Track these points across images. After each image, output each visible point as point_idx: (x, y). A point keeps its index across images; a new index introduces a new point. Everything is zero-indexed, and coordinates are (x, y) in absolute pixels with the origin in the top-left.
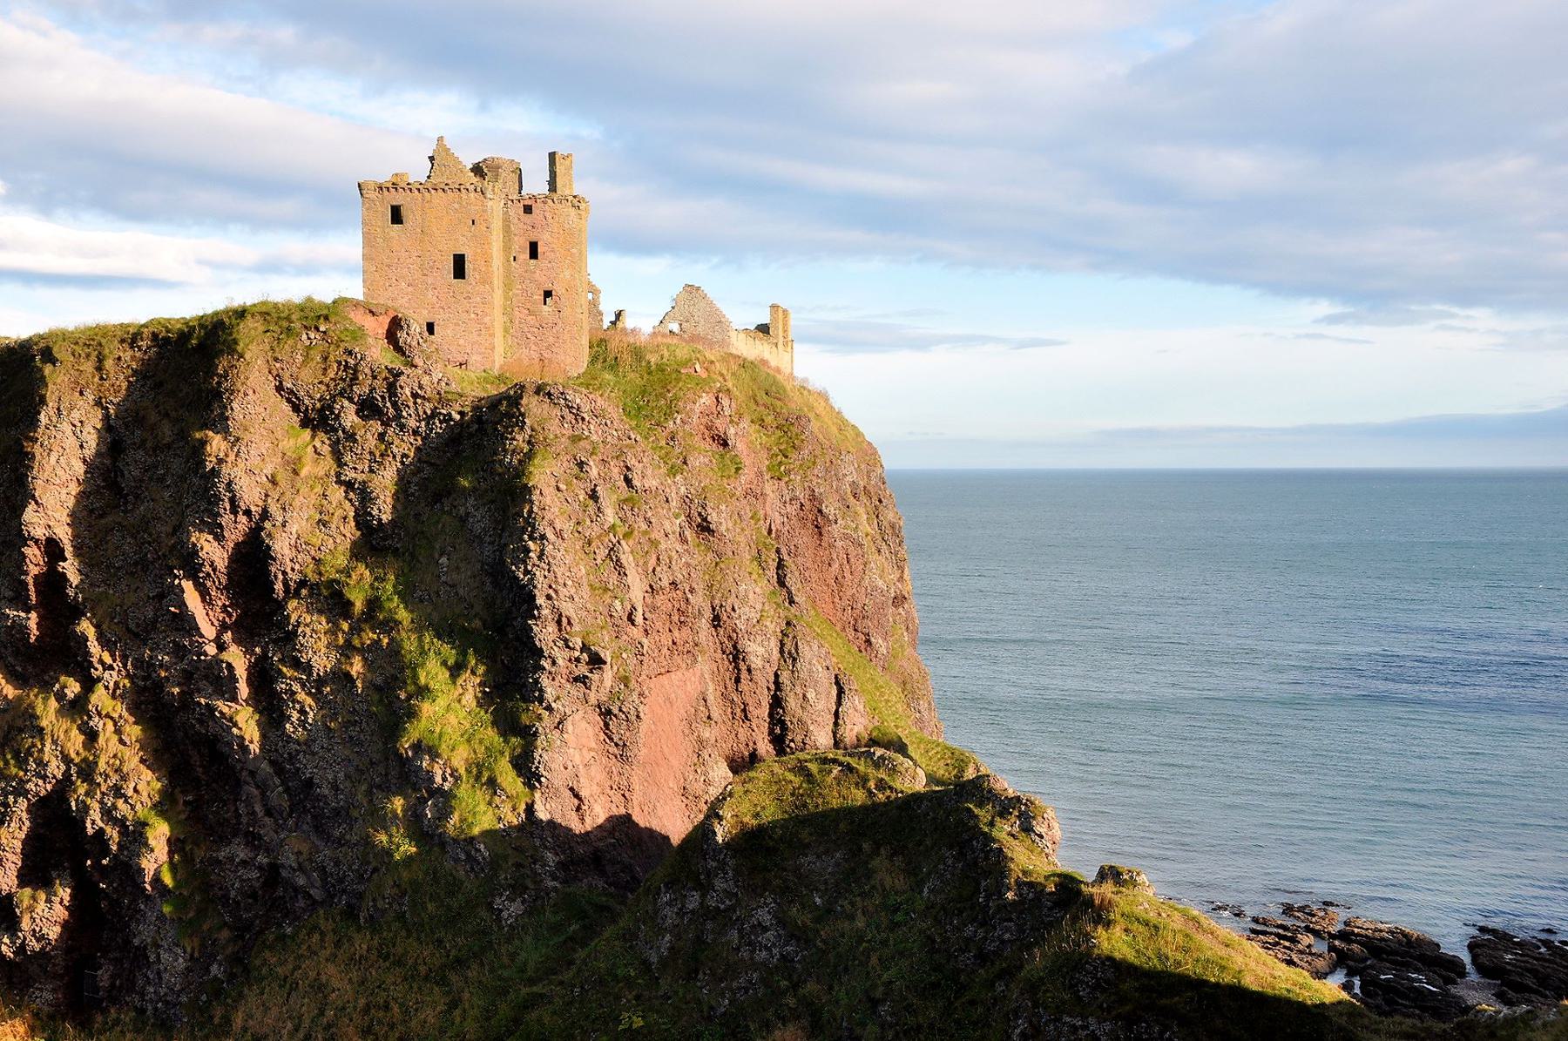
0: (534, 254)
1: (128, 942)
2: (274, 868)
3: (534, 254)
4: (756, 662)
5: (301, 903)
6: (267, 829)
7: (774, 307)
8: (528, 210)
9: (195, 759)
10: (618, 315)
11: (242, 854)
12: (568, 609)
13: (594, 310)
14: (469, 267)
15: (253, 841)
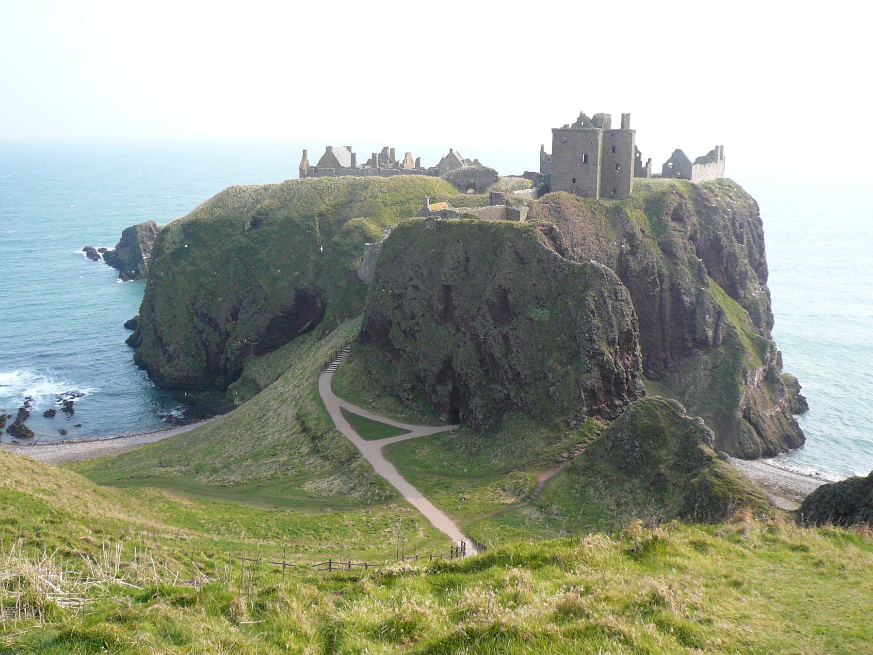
0: (614, 151)
1: (467, 407)
2: (508, 396)
3: (614, 151)
4: (687, 305)
5: (515, 406)
6: (507, 384)
7: (717, 147)
8: (612, 135)
9: (487, 358)
10: (649, 160)
11: (500, 388)
12: (595, 337)
13: (638, 160)
14: (589, 159)
15: (502, 385)
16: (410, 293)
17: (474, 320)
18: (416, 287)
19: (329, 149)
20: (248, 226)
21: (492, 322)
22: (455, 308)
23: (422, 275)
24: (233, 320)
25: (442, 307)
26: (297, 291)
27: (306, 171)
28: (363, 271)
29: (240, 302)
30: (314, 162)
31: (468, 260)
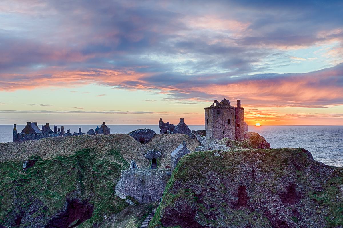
16: (210, 193)
17: (265, 204)
18: (212, 189)
19: (28, 124)
20: (25, 166)
21: (282, 204)
22: (248, 198)
23: (216, 182)
24: (16, 224)
25: (237, 199)
26: (68, 201)
27: (17, 137)
28: (120, 186)
29: (23, 213)
30: (19, 131)
31: (254, 171)
